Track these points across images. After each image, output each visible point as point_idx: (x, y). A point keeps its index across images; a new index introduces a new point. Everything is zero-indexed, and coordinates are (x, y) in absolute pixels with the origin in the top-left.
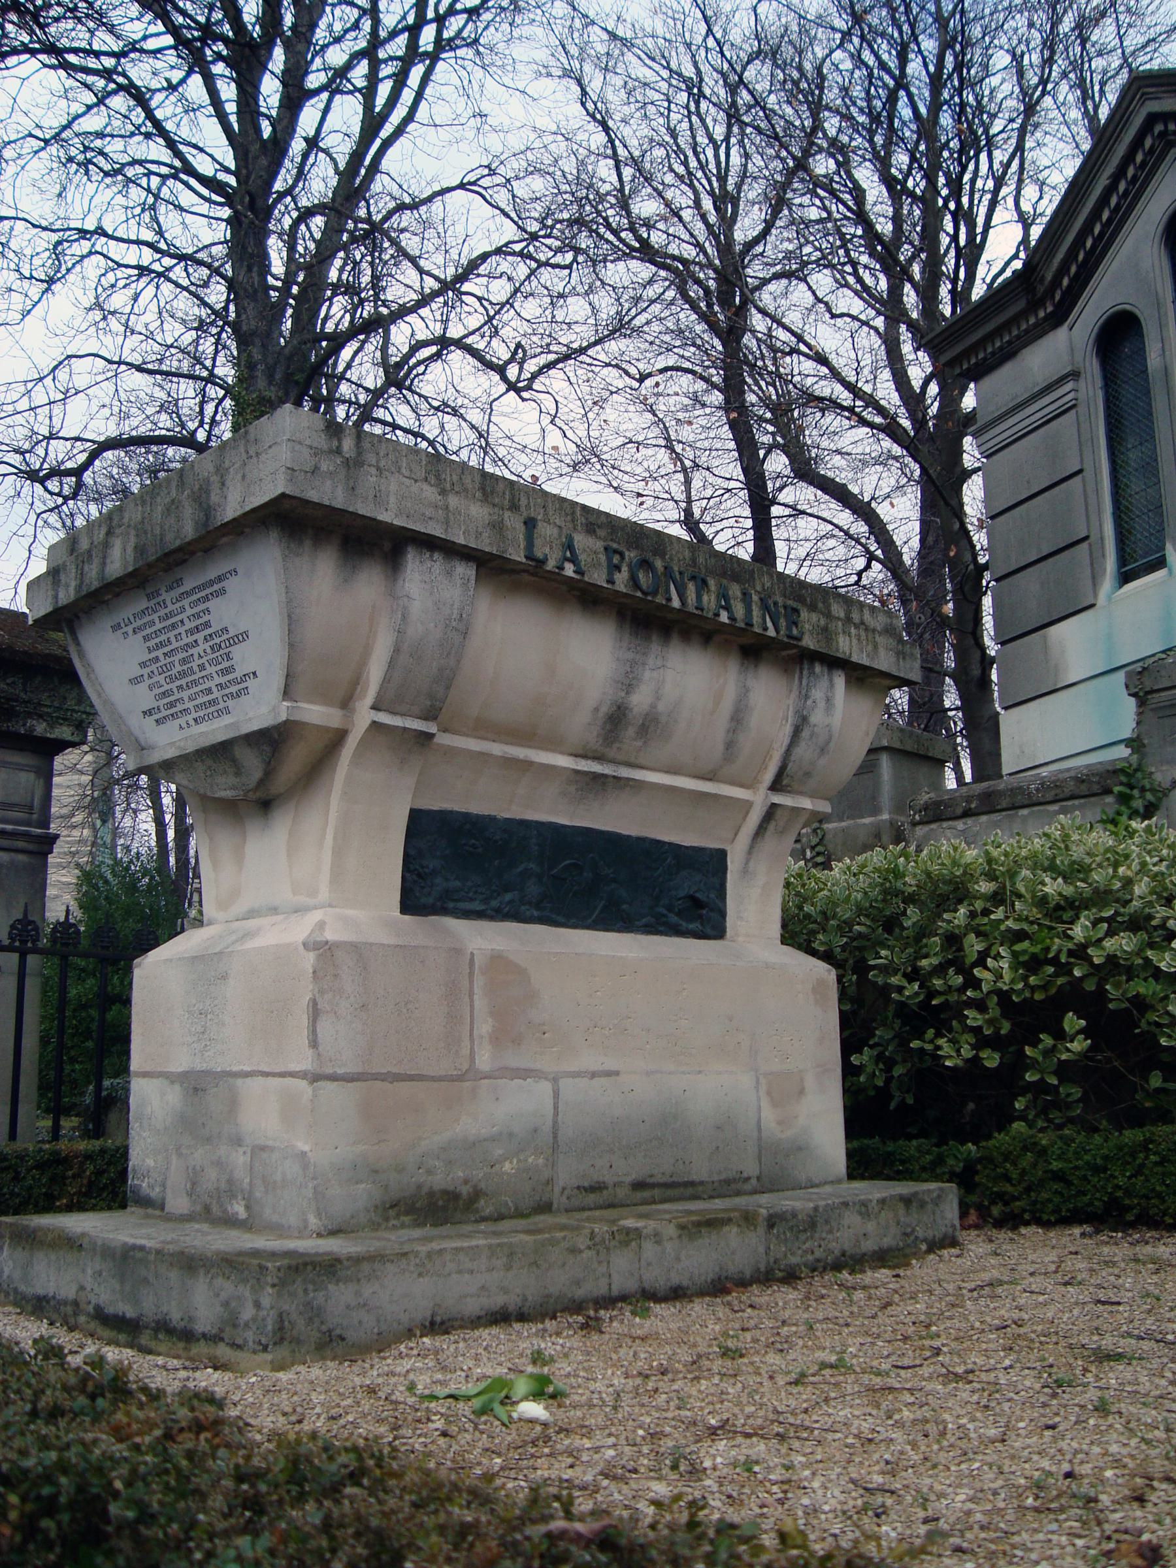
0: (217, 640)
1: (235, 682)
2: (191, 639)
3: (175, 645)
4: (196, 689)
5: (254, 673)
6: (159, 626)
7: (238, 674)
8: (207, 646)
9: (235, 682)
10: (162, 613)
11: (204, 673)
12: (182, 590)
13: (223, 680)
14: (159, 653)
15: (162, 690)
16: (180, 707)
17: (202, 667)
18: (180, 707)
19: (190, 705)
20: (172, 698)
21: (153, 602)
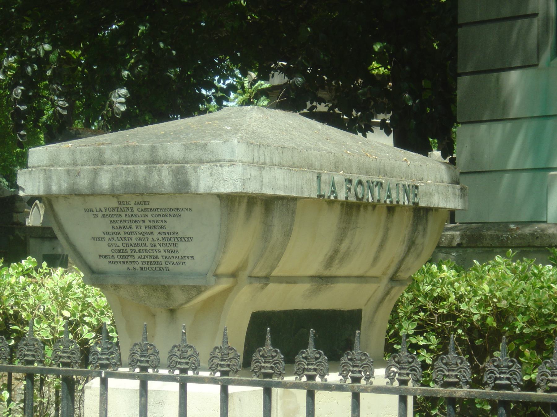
0: (169, 236)
10: (129, 213)
13: (168, 255)
14: (122, 231)
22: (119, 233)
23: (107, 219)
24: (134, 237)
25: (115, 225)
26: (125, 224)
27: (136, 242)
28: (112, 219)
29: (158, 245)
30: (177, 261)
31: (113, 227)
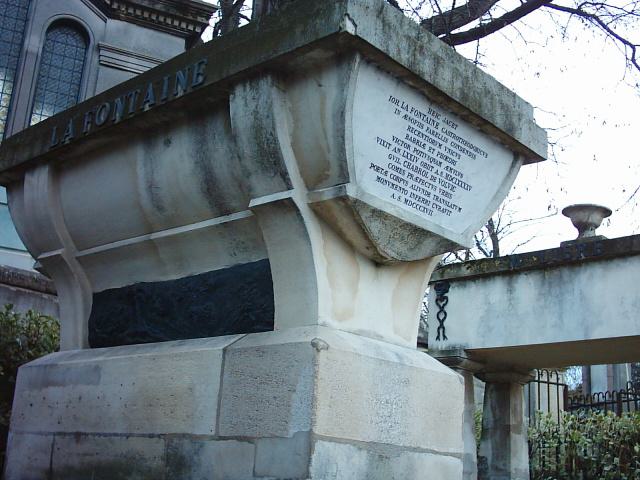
1: (447, 204)
2: (438, 159)
3: (426, 151)
6: (423, 131)
7: (451, 201)
8: (445, 172)
9: (447, 204)
10: (432, 128)
11: (432, 182)
12: (453, 130)
14: (413, 146)
15: (398, 166)
16: (401, 185)
18: (401, 185)
19: (410, 190)
20: (400, 176)
21: (430, 116)
24: (421, 159)
25: (411, 135)
26: (421, 139)
28: (412, 125)
29: (437, 180)
31: (408, 136)
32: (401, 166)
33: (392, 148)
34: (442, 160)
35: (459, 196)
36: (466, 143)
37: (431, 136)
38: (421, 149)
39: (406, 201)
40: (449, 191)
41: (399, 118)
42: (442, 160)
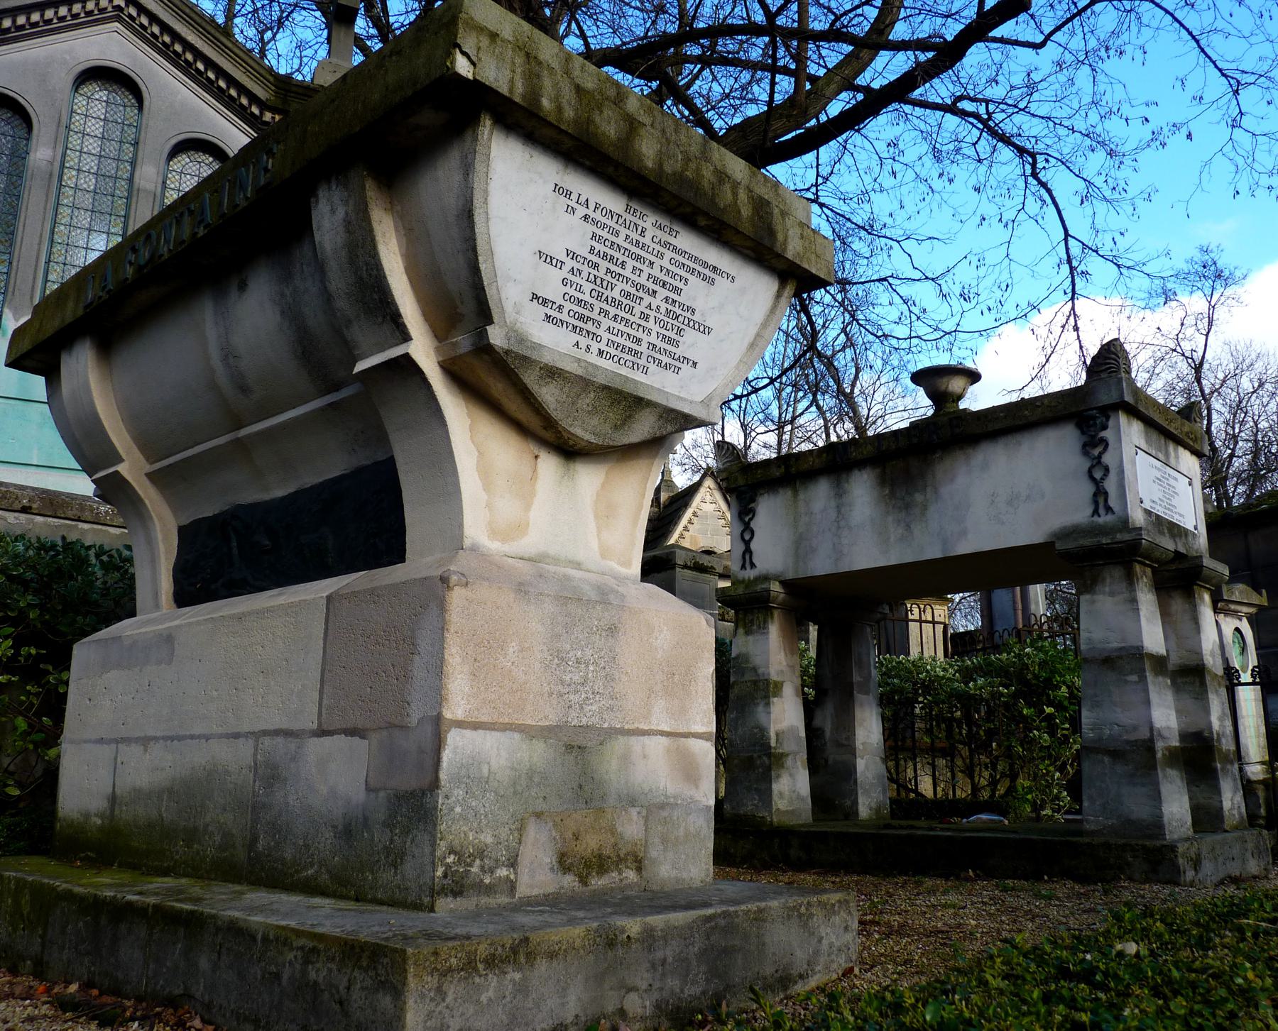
0: (679, 312)
1: (672, 355)
4: (622, 327)
5: (695, 364)
6: (620, 241)
7: (678, 352)
8: (664, 306)
10: (635, 236)
11: (643, 323)
13: (659, 344)
14: (604, 265)
15: (581, 296)
16: (589, 326)
17: (645, 317)
19: (606, 336)
20: (586, 313)
21: (629, 217)
22: (596, 266)
23: (592, 228)
24: (620, 286)
25: (598, 247)
26: (616, 255)
27: (618, 297)
28: (599, 232)
29: (652, 320)
30: (670, 361)
31: (592, 250)
32: (586, 297)
33: (567, 268)
34: (656, 288)
35: (691, 343)
36: (696, 260)
37: (634, 249)
38: (618, 270)
39: (601, 352)
40: (673, 336)
41: (575, 220)
42: (656, 288)
